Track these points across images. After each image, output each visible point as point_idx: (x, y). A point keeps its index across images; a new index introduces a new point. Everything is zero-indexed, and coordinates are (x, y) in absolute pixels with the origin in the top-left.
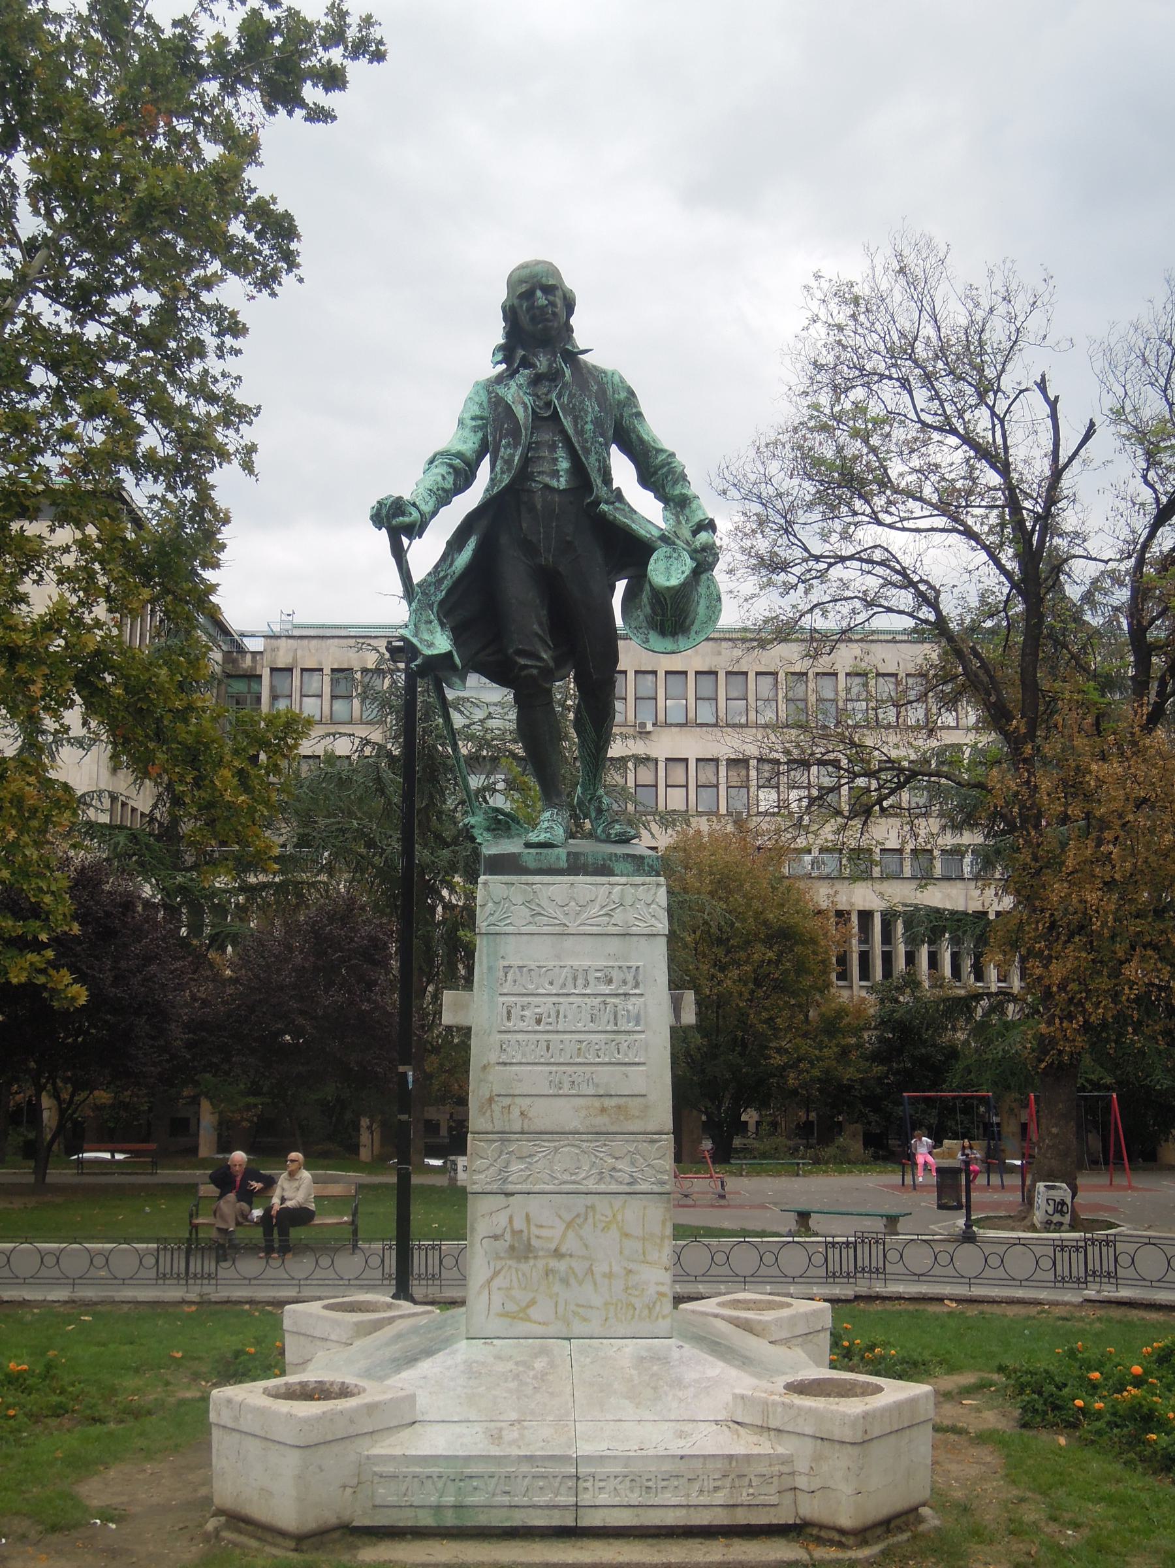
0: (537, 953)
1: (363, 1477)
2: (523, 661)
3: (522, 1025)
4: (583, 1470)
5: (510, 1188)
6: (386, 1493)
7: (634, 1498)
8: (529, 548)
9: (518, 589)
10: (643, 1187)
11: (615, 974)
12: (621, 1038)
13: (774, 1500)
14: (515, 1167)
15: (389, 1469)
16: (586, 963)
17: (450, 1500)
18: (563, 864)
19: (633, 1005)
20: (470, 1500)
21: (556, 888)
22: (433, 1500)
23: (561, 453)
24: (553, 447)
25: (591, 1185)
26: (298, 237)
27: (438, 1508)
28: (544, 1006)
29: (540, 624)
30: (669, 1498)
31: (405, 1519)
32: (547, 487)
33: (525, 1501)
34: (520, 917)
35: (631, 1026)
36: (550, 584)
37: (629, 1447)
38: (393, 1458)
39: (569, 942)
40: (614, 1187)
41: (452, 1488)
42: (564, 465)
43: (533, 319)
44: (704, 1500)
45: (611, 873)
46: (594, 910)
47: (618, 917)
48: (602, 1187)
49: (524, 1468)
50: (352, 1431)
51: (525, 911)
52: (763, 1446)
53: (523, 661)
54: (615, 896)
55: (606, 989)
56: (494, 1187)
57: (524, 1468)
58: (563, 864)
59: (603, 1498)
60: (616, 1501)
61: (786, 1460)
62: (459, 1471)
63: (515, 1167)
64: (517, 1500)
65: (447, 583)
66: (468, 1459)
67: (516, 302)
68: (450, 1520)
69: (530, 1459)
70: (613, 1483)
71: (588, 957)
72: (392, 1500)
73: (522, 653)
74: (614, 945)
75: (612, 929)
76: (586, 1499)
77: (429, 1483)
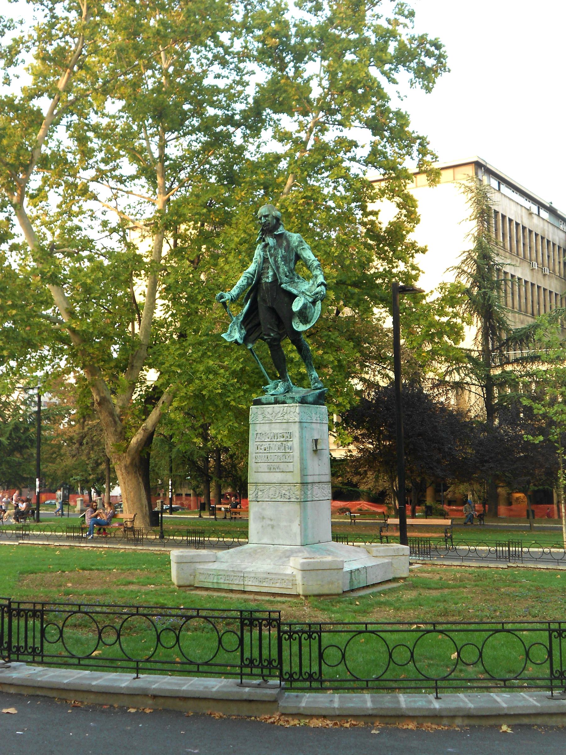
0: (265, 428)
3: (261, 451)
5: (259, 500)
7: (257, 584)
8: (264, 301)
11: (285, 435)
13: (291, 587)
15: (202, 572)
16: (277, 431)
17: (215, 581)
18: (273, 401)
19: (290, 444)
22: (211, 581)
25: (279, 499)
26: (427, 35)
28: (266, 445)
29: (271, 325)
30: (265, 584)
34: (260, 419)
35: (289, 451)
39: (273, 425)
41: (216, 577)
44: (273, 585)
46: (279, 415)
47: (286, 417)
48: (282, 500)
49: (232, 574)
50: (192, 560)
51: (261, 416)
56: (254, 499)
57: (232, 574)
58: (273, 401)
59: (250, 583)
63: (260, 493)
64: (230, 582)
68: (216, 587)
69: (233, 571)
70: (252, 579)
71: (278, 429)
72: (203, 580)
74: (285, 426)
75: (284, 421)
76: (246, 583)
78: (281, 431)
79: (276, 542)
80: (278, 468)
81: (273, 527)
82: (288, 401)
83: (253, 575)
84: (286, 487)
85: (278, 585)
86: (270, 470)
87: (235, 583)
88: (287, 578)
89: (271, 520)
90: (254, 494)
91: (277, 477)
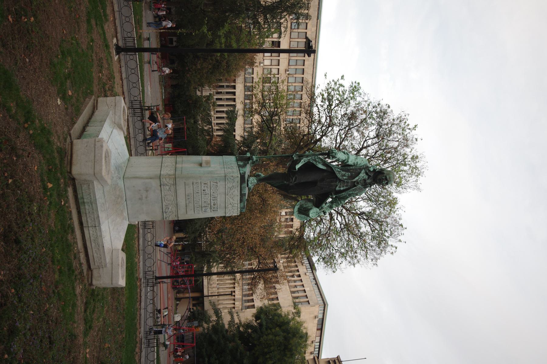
1: (89, 184)
2: (294, 179)
3: (203, 187)
4: (97, 228)
5: (162, 187)
6: (85, 187)
7: (92, 238)
9: (311, 177)
10: (165, 214)
11: (216, 206)
12: (200, 208)
13: (96, 264)
14: (167, 187)
15: (91, 187)
16: (218, 200)
17: (85, 201)
18: (243, 193)
19: (209, 210)
20: (86, 205)
21: (237, 192)
22: (85, 197)
23: (345, 188)
24: (347, 186)
25: (164, 204)
27: (83, 198)
28: (208, 191)
30: (93, 245)
31: (79, 191)
32: (337, 186)
33: (88, 216)
35: (203, 210)
36: (313, 183)
37: (104, 234)
38: (94, 188)
40: (164, 209)
42: (342, 189)
43: (380, 179)
44: (94, 252)
45: (241, 202)
46: (231, 201)
47: (230, 206)
48: (164, 206)
51: (231, 186)
52: (108, 260)
53: (294, 179)
54: (235, 205)
55: (212, 204)
58: (243, 193)
59: (91, 232)
60: (91, 235)
61: (106, 266)
62: (93, 203)
63: (167, 187)
64: (88, 215)
65: (314, 162)
66: (96, 204)
67: (385, 175)
68: (80, 201)
70: (95, 234)
71: (220, 200)
72: (83, 188)
73: (296, 178)
74: (223, 205)
76: (91, 229)
77: (89, 196)
78: (219, 203)
79: (128, 202)
80: (190, 202)
81: (141, 199)
82: (242, 204)
83: (98, 235)
84: (174, 209)
85: (95, 255)
86: (187, 196)
87: (89, 220)
88: (103, 261)
89: (146, 198)
90: (166, 182)
91: (182, 201)
